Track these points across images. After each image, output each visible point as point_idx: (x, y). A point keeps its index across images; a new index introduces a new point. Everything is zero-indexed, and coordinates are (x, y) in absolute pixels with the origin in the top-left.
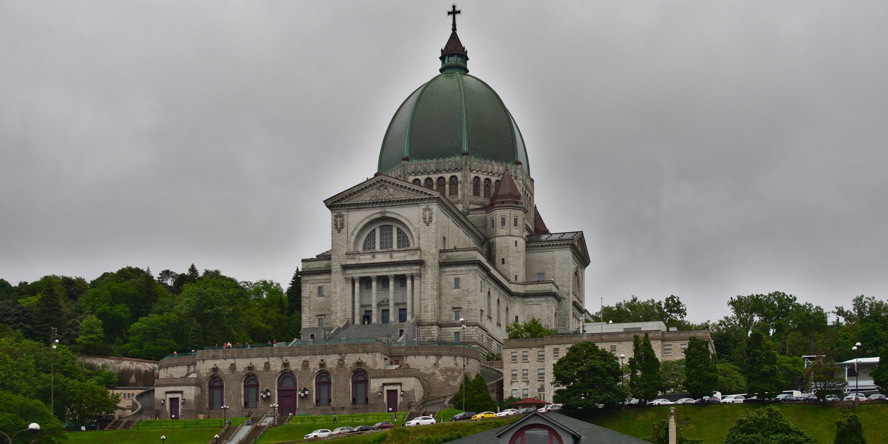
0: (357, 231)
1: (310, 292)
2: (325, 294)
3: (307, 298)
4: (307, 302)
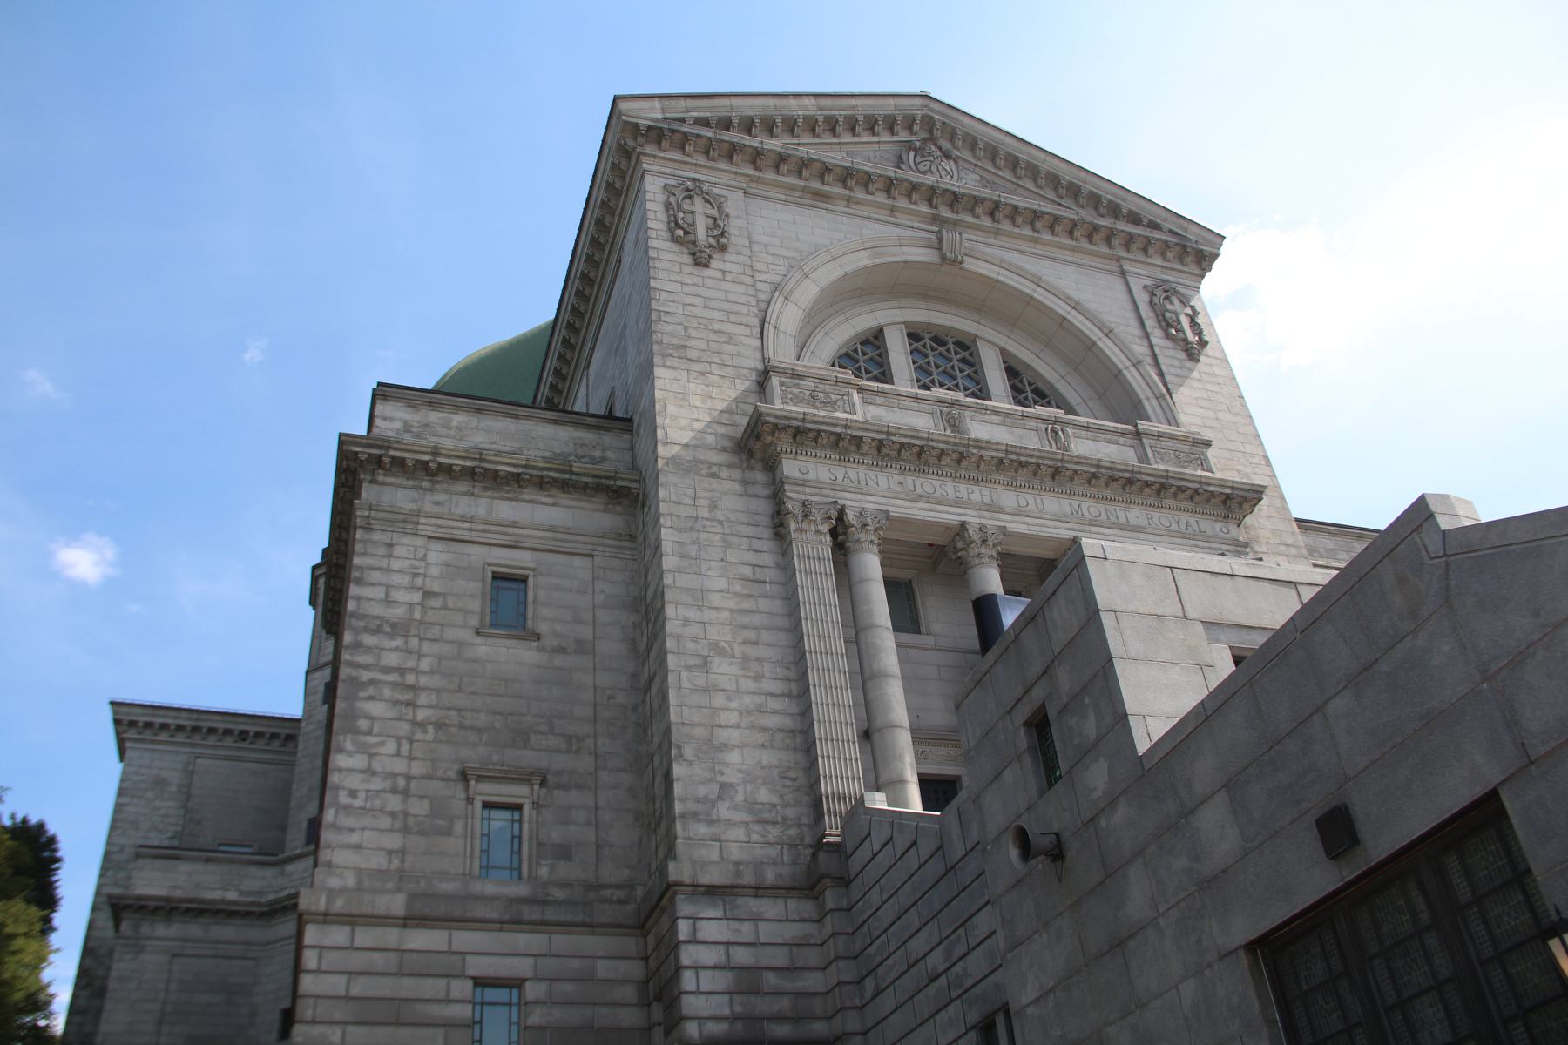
0: (808, 292)
1: (428, 594)
2: (543, 628)
3: (399, 628)
4: (392, 659)
